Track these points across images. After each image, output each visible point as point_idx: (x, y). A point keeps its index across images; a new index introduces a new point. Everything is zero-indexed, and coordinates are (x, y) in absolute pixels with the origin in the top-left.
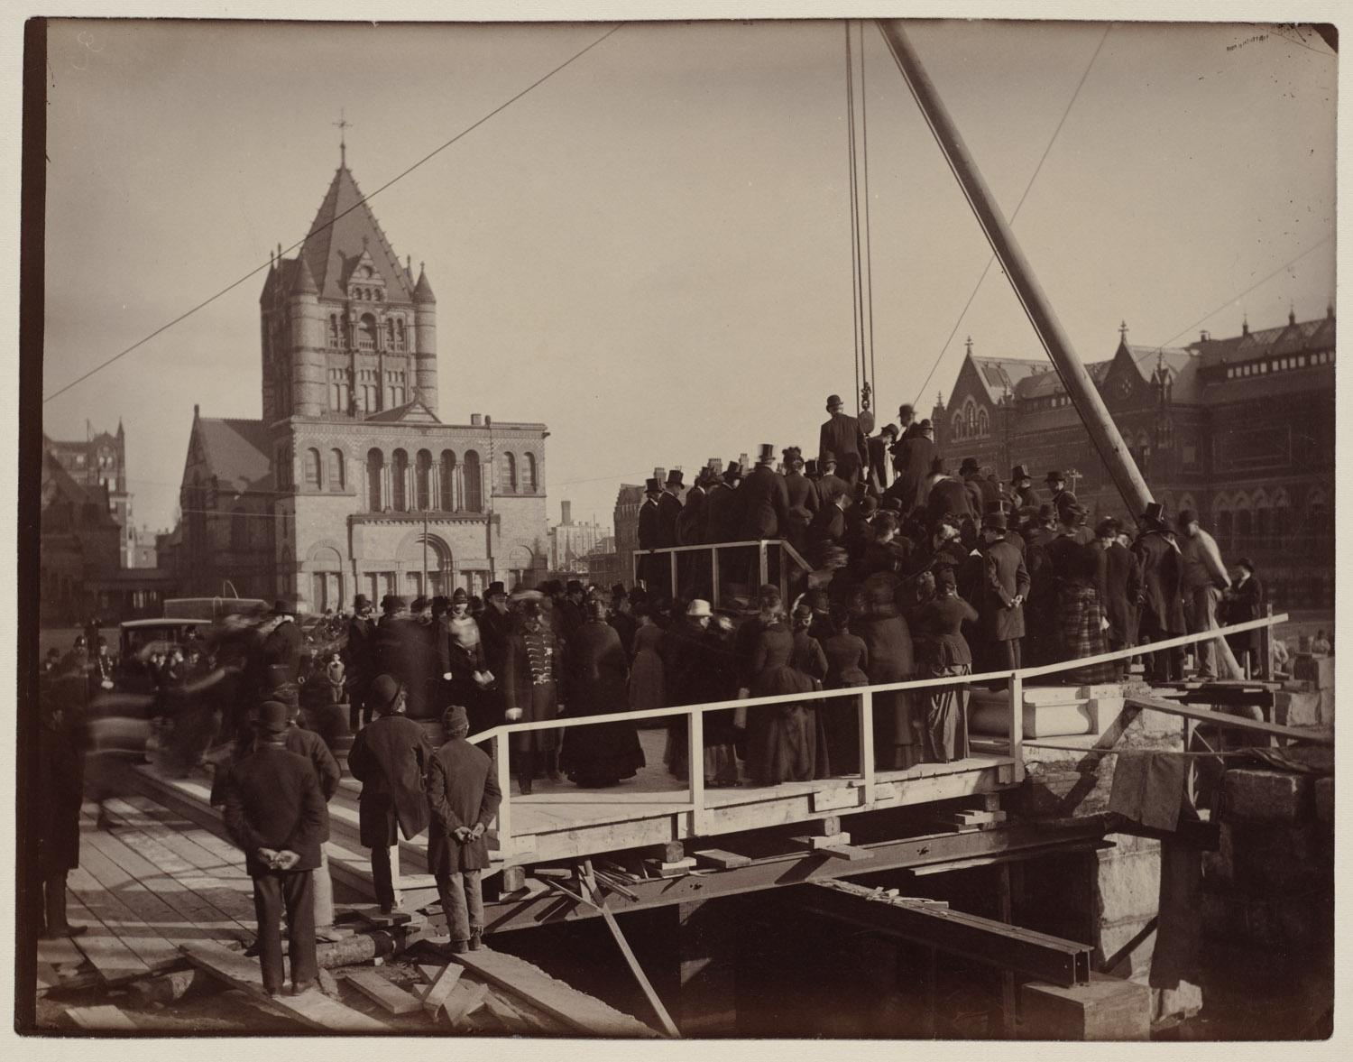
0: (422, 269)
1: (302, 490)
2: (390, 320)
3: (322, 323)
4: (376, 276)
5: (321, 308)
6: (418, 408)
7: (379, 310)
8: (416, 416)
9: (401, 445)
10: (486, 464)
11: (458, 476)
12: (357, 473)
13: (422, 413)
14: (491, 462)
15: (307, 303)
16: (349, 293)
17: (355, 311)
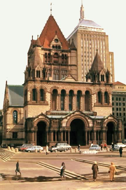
1: (29, 103)
2: (63, 55)
3: (43, 55)
4: (59, 42)
5: (42, 51)
6: (59, 43)
7: (60, 52)
8: (69, 79)
9: (64, 88)
10: (92, 95)
11: (82, 100)
12: (48, 97)
13: (71, 78)
14: (94, 95)
15: (38, 49)
17: (52, 52)
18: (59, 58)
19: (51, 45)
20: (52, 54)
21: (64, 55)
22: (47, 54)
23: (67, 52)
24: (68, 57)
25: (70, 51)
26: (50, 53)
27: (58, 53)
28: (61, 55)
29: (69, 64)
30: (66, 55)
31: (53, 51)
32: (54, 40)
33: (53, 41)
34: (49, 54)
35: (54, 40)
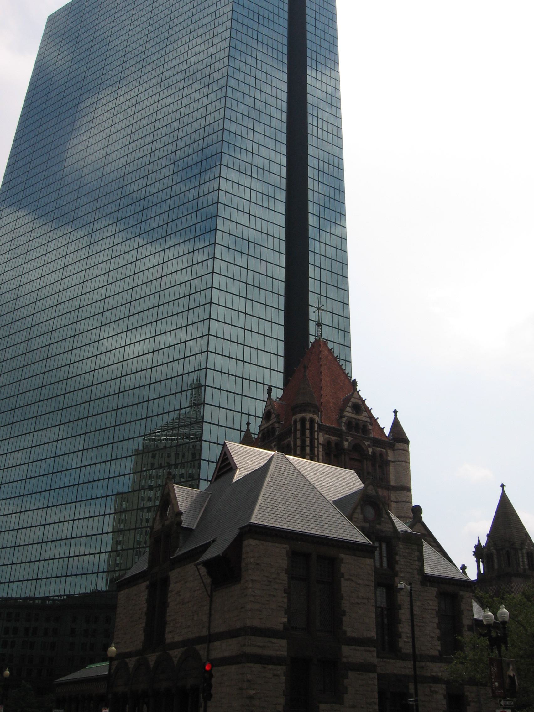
0: (396, 415)
7: (367, 443)
16: (343, 424)
18: (365, 461)
19: (344, 420)
20: (346, 444)
21: (378, 455)
22: (333, 445)
23: (384, 448)
24: (390, 461)
25: (394, 445)
27: (363, 446)
28: (370, 450)
29: (392, 483)
30: (381, 455)
31: (350, 439)
32: (350, 404)
33: (348, 409)
34: (338, 445)
35: (350, 404)
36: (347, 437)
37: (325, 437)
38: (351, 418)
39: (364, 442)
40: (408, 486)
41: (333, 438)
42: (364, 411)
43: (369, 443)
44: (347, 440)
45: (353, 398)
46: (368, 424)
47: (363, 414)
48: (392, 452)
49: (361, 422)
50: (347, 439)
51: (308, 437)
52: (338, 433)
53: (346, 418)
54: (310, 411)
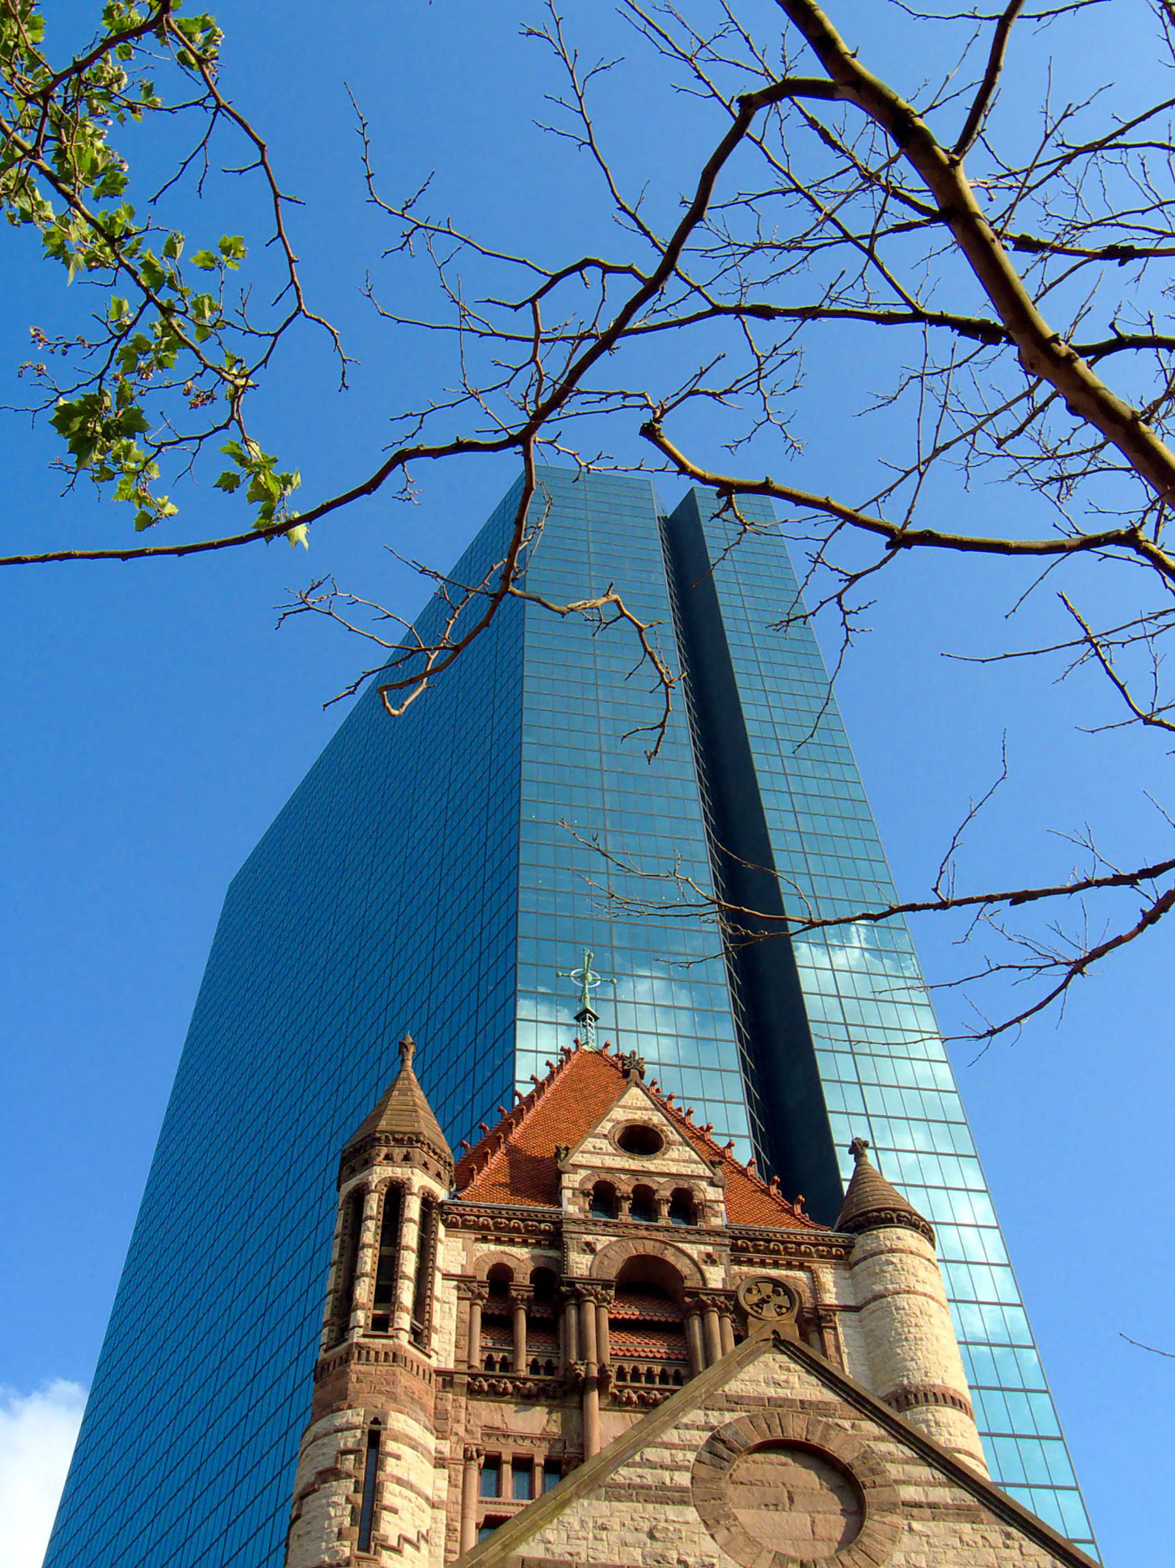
7: (693, 1250)
16: (567, 1194)
20: (580, 1264)
22: (523, 1278)
23: (801, 1267)
25: (849, 1247)
26: (561, 1263)
31: (602, 1242)
32: (606, 1126)
36: (589, 1238)
37: (478, 1254)
38: (610, 1170)
39: (680, 1245)
40: (938, 1382)
41: (522, 1253)
42: (673, 1143)
43: (710, 1249)
44: (590, 1248)
45: (624, 1107)
46: (704, 1184)
47: (674, 1153)
48: (847, 1274)
49: (662, 1180)
50: (588, 1244)
51: (370, 1246)
52: (542, 1226)
53: (583, 1173)
54: (388, 1157)
